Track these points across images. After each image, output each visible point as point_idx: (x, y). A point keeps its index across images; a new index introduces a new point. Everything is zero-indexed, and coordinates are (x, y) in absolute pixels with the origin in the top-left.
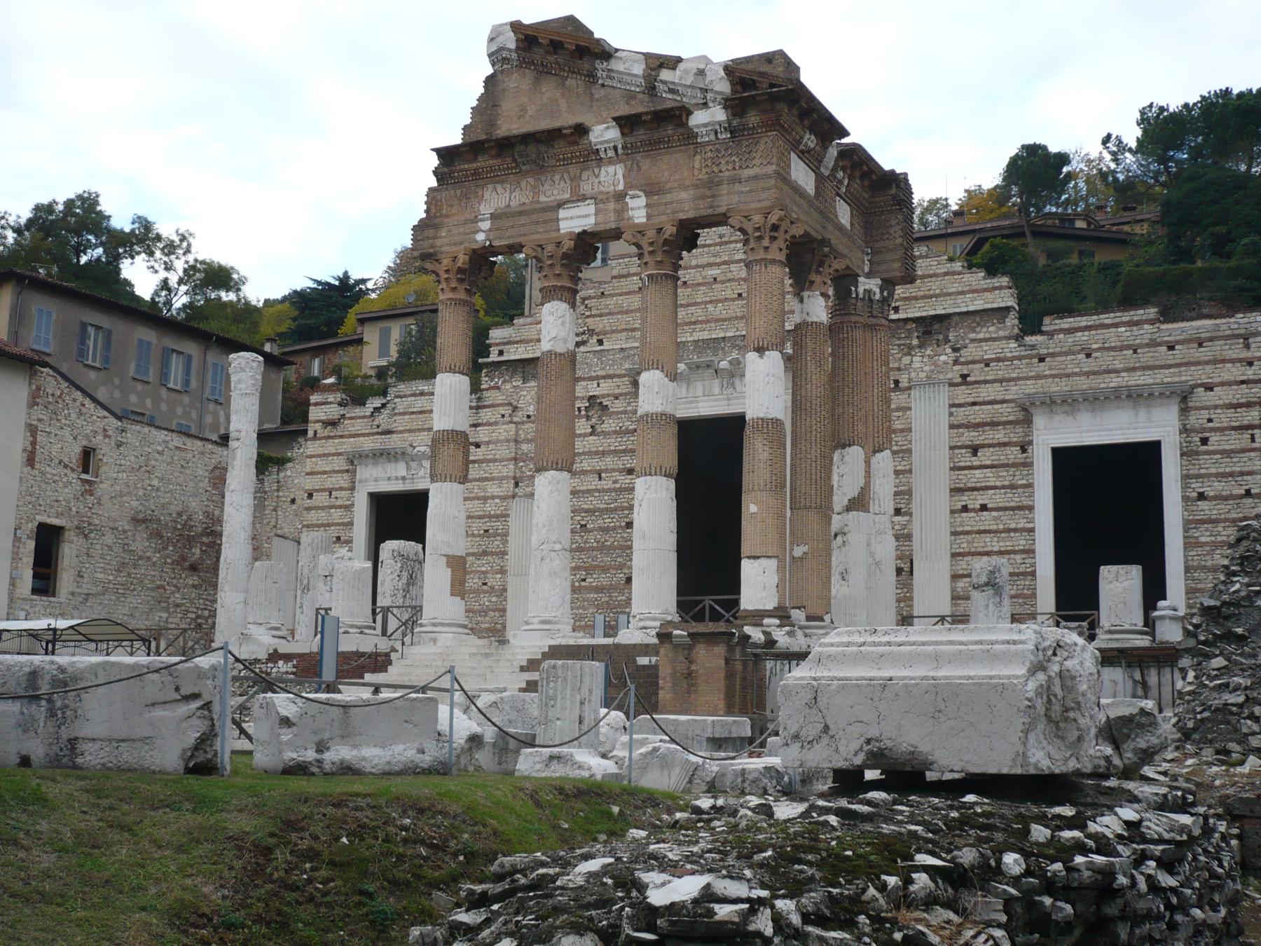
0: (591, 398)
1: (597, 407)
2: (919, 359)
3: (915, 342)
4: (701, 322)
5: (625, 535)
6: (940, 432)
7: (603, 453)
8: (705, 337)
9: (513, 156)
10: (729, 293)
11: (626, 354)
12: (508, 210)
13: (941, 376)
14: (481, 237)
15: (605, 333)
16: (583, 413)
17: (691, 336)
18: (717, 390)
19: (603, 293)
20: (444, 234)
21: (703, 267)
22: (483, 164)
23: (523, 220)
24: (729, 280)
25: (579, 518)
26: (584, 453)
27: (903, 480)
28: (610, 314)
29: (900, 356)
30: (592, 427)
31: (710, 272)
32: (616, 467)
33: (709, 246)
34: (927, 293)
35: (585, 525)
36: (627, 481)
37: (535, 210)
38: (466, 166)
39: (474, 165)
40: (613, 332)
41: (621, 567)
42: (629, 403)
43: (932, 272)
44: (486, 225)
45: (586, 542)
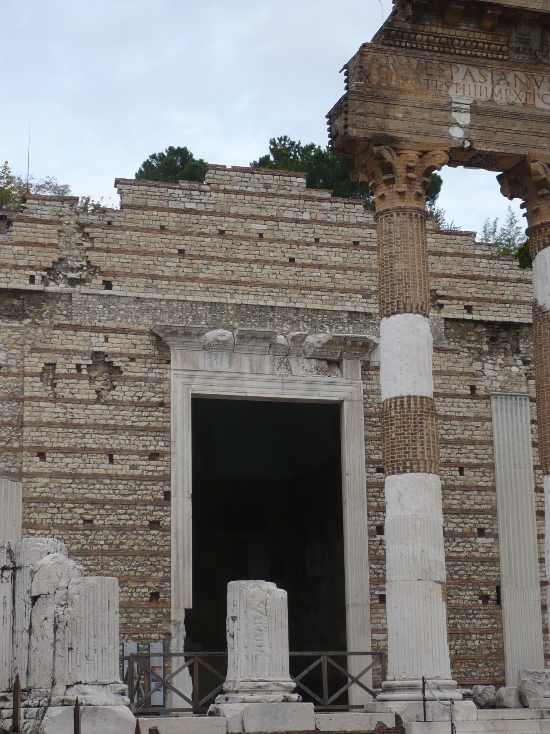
0: (96, 354)
1: (101, 368)
2: (491, 367)
3: (486, 348)
4: (245, 284)
5: (150, 538)
6: (524, 450)
7: (115, 429)
8: (250, 302)
9: (509, 36)
10: (277, 255)
11: (144, 305)
12: (492, 106)
13: (515, 389)
14: (457, 133)
15: (115, 275)
16: (84, 372)
17: (232, 297)
18: (267, 369)
19: (109, 223)
20: (400, 115)
21: (246, 217)
22: (465, 34)
23: (519, 126)
24: (279, 240)
25: (82, 511)
26: (87, 426)
27: (486, 497)
28: (120, 251)
29: (471, 359)
30: (97, 392)
31: (254, 226)
32: (135, 448)
33: (252, 194)
34: (500, 297)
35: (91, 521)
36: (151, 468)
37: (535, 116)
38: (440, 30)
39: (453, 32)
40: (126, 275)
41: (143, 579)
42: (151, 369)
43: (504, 276)
44: (465, 119)
45: (92, 544)
